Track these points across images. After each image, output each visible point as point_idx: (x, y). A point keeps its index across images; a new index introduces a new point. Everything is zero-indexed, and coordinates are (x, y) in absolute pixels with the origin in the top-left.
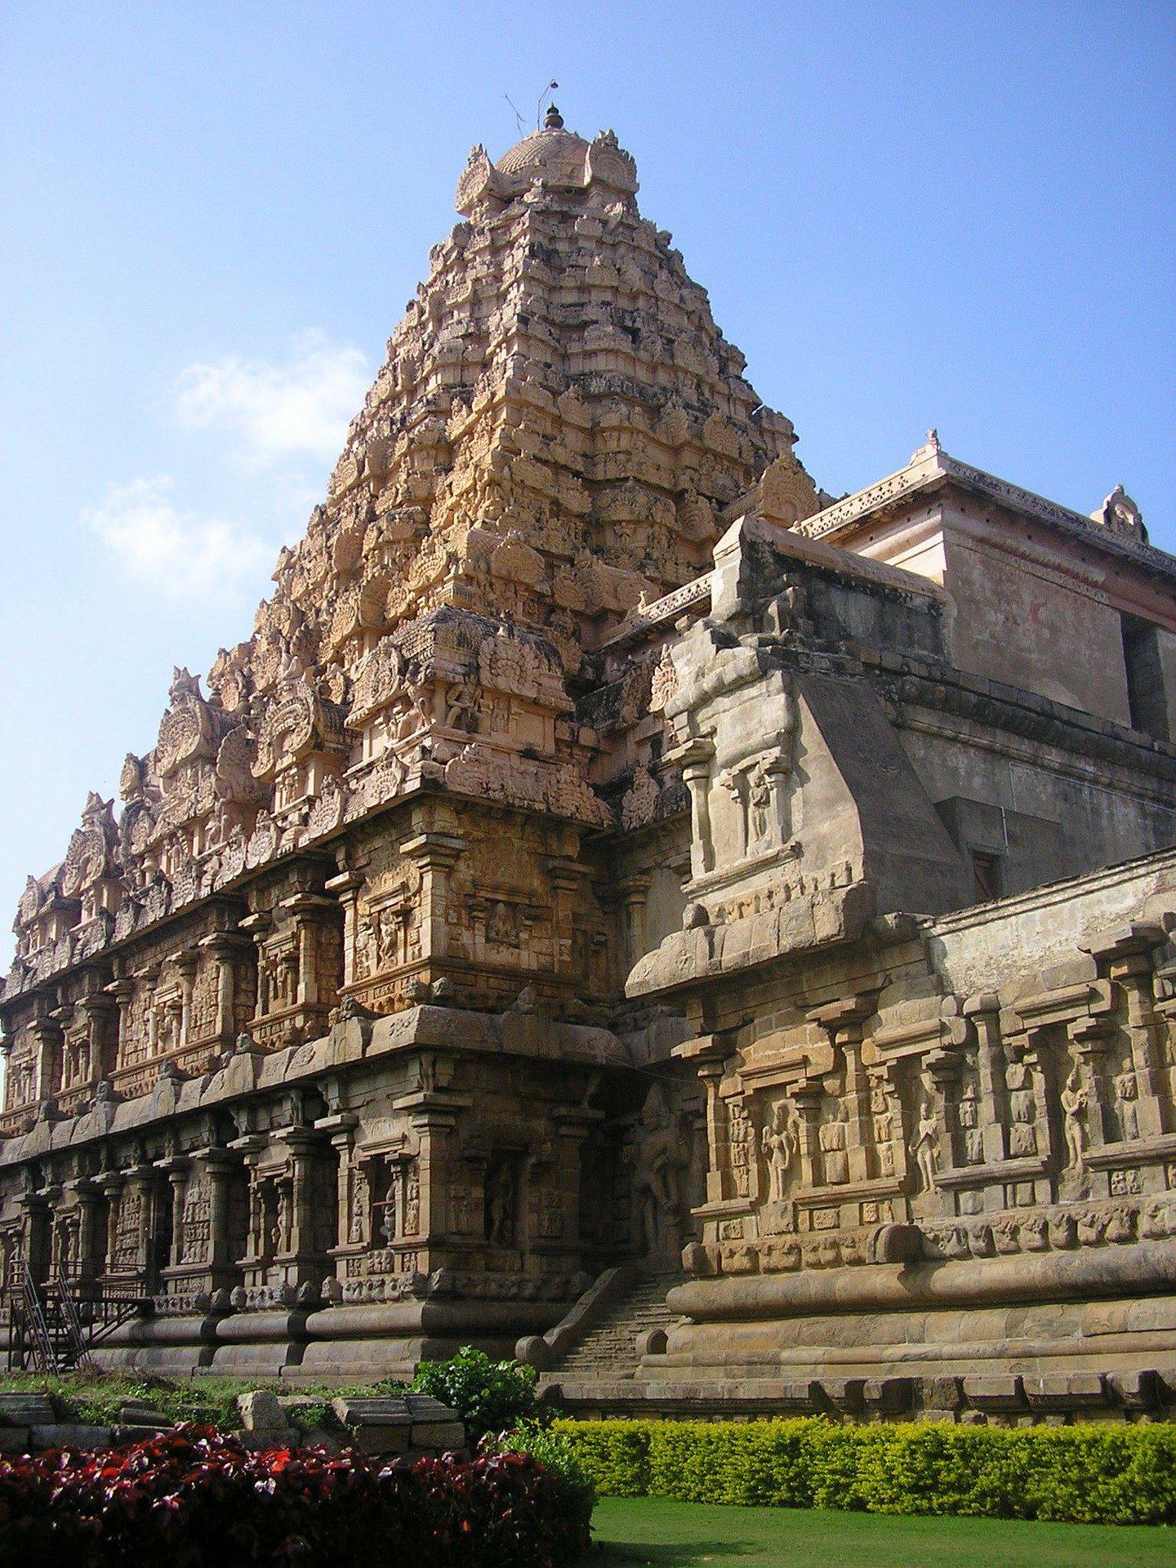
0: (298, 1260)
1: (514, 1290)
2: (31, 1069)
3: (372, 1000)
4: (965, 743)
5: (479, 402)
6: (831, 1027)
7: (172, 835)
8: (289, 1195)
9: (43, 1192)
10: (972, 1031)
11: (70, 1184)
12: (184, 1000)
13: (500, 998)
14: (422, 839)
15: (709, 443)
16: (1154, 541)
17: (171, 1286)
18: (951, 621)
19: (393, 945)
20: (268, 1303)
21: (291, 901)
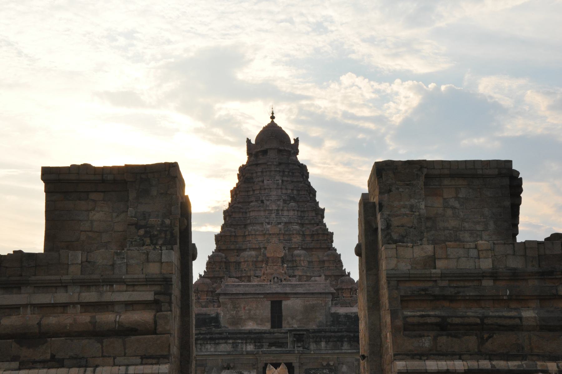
15: (271, 232)
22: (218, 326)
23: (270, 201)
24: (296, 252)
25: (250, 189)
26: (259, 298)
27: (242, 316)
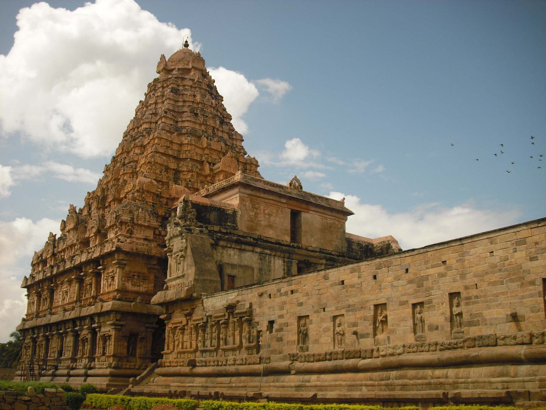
0: (88, 357)
1: (133, 367)
2: (33, 303)
3: (105, 297)
4: (234, 248)
5: (151, 137)
6: (186, 315)
7: (68, 248)
8: (87, 342)
9: (35, 336)
10: (207, 319)
11: (41, 334)
12: (68, 291)
13: (134, 299)
14: (116, 261)
15: (213, 148)
16: (304, 189)
17: (62, 362)
18: (239, 216)
19: (110, 285)
20: (81, 367)
21: (90, 271)
22: (235, 228)
27: (261, 221)
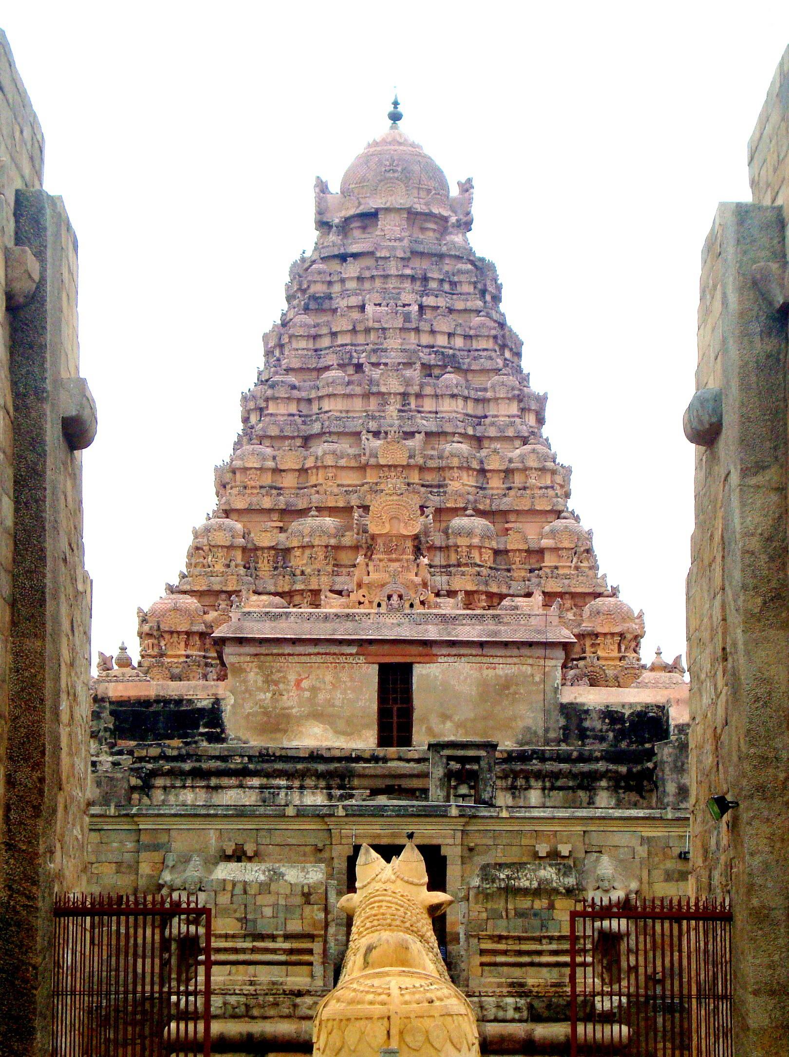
15: (382, 462)
23: (382, 367)
24: (458, 522)
25: (324, 331)
26: (343, 654)
27: (292, 708)
